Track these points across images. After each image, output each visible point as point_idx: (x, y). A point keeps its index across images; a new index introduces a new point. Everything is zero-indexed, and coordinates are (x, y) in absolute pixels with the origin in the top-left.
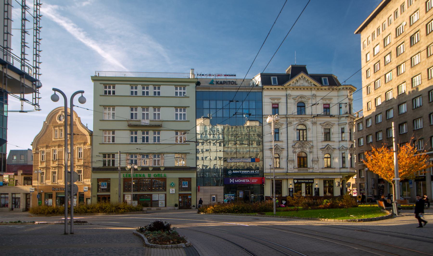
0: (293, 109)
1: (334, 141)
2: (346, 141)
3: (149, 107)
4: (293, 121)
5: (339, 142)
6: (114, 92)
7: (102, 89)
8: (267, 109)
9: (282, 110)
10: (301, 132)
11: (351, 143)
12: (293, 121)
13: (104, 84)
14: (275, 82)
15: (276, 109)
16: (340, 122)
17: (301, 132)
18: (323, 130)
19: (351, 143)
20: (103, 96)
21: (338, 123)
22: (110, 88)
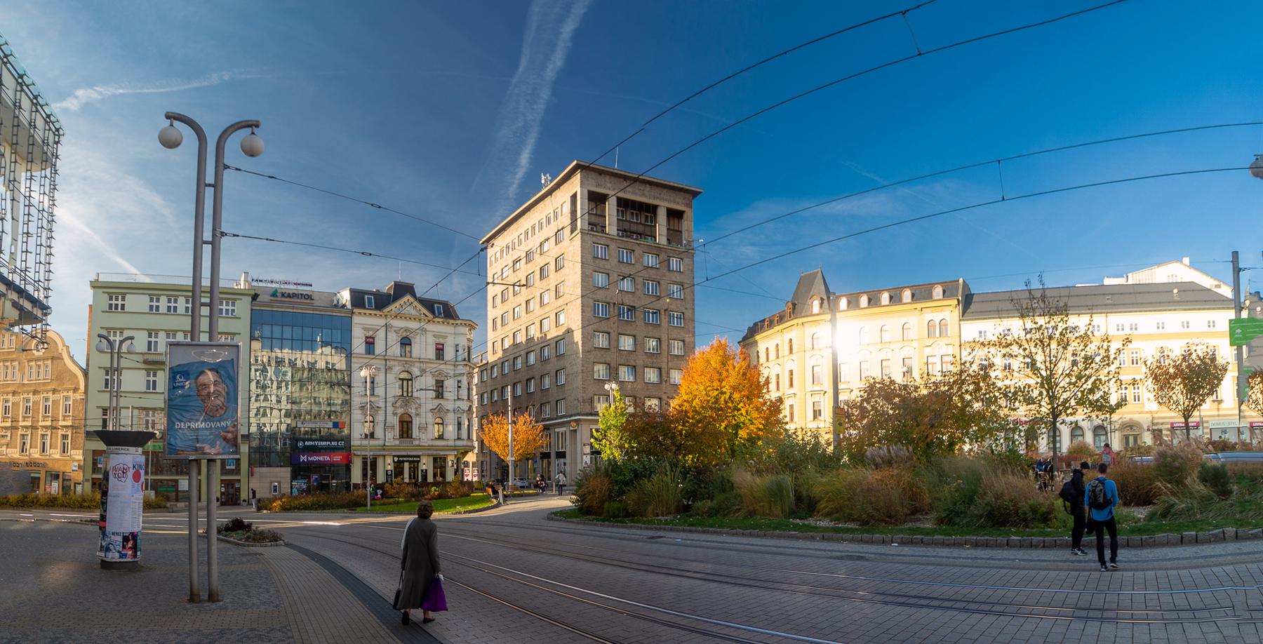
0: (396, 350)
1: (448, 400)
2: (463, 400)
3: (176, 331)
4: (395, 365)
5: (455, 400)
6: (123, 306)
7: (105, 301)
8: (358, 345)
9: (379, 348)
10: (405, 382)
11: (469, 404)
12: (395, 365)
13: (108, 293)
14: (370, 305)
15: (371, 346)
16: (456, 372)
17: (405, 382)
18: (434, 382)
19: (469, 404)
20: (107, 312)
21: (453, 372)
22: (117, 299)
